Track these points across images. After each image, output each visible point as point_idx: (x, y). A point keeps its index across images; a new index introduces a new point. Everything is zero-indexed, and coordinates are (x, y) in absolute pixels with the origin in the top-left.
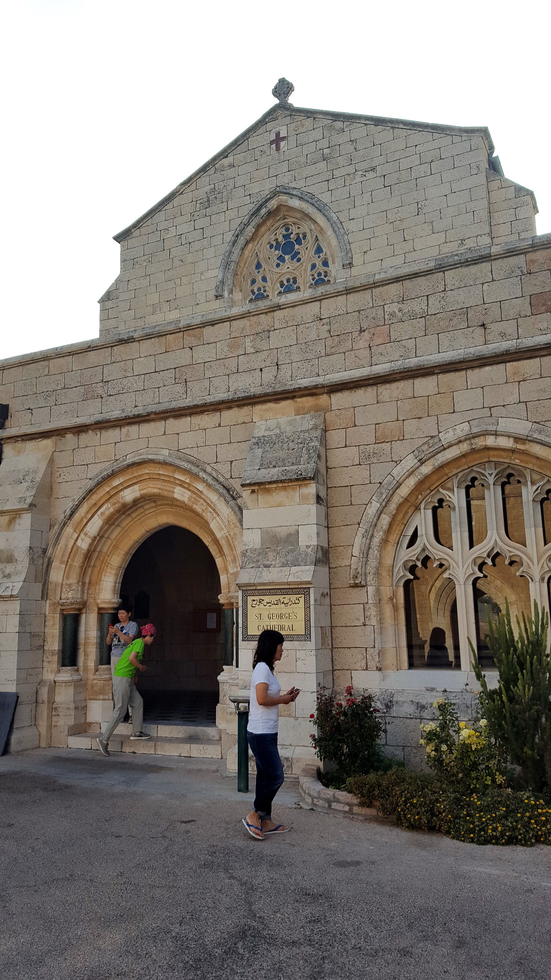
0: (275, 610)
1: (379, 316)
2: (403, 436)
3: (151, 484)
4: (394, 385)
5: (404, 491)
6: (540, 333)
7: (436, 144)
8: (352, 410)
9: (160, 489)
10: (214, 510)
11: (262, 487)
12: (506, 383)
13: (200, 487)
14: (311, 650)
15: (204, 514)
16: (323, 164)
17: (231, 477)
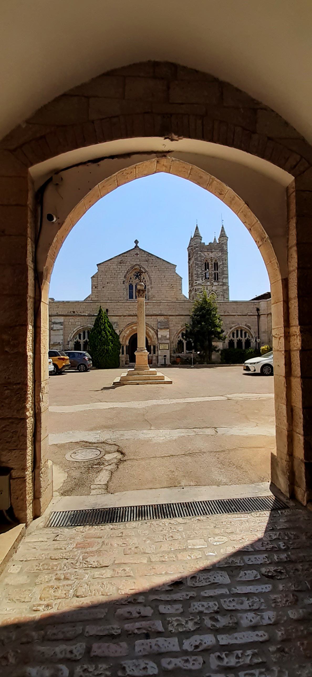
7: (168, 265)
13: (148, 327)
16: (146, 262)
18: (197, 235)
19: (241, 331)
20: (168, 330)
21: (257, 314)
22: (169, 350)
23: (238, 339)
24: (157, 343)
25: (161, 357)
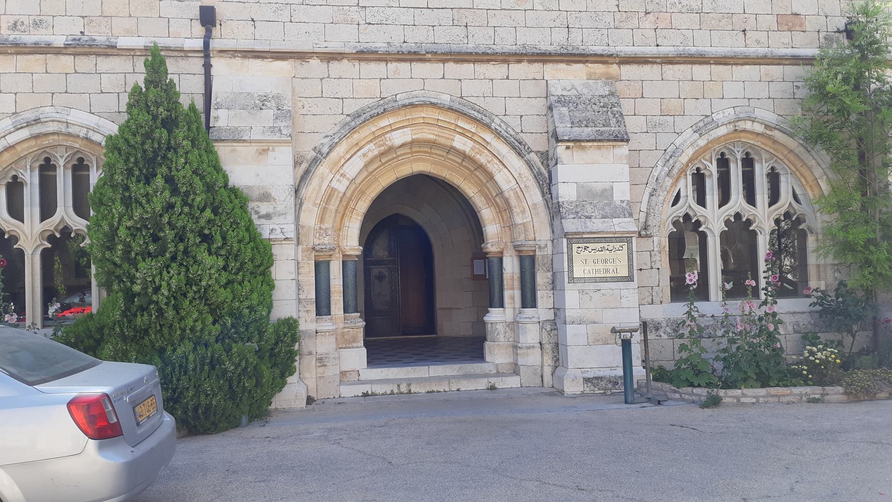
1: (662, 3)
2: (684, 112)
3: (426, 129)
4: (676, 67)
5: (684, 159)
6: (783, 46)
8: (640, 83)
9: (436, 135)
10: (500, 161)
11: (578, 144)
12: (760, 81)
13: (488, 137)
14: (634, 289)
15: (488, 165)
17: (522, 131)
20: (623, 150)
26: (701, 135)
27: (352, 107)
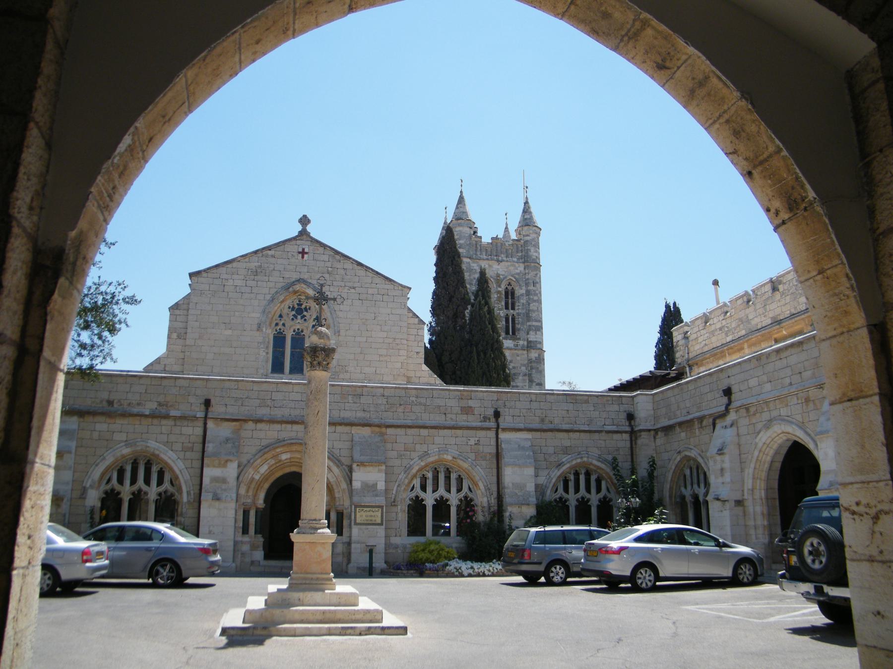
0: (369, 514)
4: (413, 430)
5: (414, 471)
7: (387, 287)
18: (461, 215)
19: (588, 474)
21: (628, 429)
22: (383, 527)
23: (579, 495)
24: (347, 503)
25: (358, 546)
26: (422, 461)
27: (264, 443)
